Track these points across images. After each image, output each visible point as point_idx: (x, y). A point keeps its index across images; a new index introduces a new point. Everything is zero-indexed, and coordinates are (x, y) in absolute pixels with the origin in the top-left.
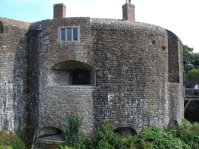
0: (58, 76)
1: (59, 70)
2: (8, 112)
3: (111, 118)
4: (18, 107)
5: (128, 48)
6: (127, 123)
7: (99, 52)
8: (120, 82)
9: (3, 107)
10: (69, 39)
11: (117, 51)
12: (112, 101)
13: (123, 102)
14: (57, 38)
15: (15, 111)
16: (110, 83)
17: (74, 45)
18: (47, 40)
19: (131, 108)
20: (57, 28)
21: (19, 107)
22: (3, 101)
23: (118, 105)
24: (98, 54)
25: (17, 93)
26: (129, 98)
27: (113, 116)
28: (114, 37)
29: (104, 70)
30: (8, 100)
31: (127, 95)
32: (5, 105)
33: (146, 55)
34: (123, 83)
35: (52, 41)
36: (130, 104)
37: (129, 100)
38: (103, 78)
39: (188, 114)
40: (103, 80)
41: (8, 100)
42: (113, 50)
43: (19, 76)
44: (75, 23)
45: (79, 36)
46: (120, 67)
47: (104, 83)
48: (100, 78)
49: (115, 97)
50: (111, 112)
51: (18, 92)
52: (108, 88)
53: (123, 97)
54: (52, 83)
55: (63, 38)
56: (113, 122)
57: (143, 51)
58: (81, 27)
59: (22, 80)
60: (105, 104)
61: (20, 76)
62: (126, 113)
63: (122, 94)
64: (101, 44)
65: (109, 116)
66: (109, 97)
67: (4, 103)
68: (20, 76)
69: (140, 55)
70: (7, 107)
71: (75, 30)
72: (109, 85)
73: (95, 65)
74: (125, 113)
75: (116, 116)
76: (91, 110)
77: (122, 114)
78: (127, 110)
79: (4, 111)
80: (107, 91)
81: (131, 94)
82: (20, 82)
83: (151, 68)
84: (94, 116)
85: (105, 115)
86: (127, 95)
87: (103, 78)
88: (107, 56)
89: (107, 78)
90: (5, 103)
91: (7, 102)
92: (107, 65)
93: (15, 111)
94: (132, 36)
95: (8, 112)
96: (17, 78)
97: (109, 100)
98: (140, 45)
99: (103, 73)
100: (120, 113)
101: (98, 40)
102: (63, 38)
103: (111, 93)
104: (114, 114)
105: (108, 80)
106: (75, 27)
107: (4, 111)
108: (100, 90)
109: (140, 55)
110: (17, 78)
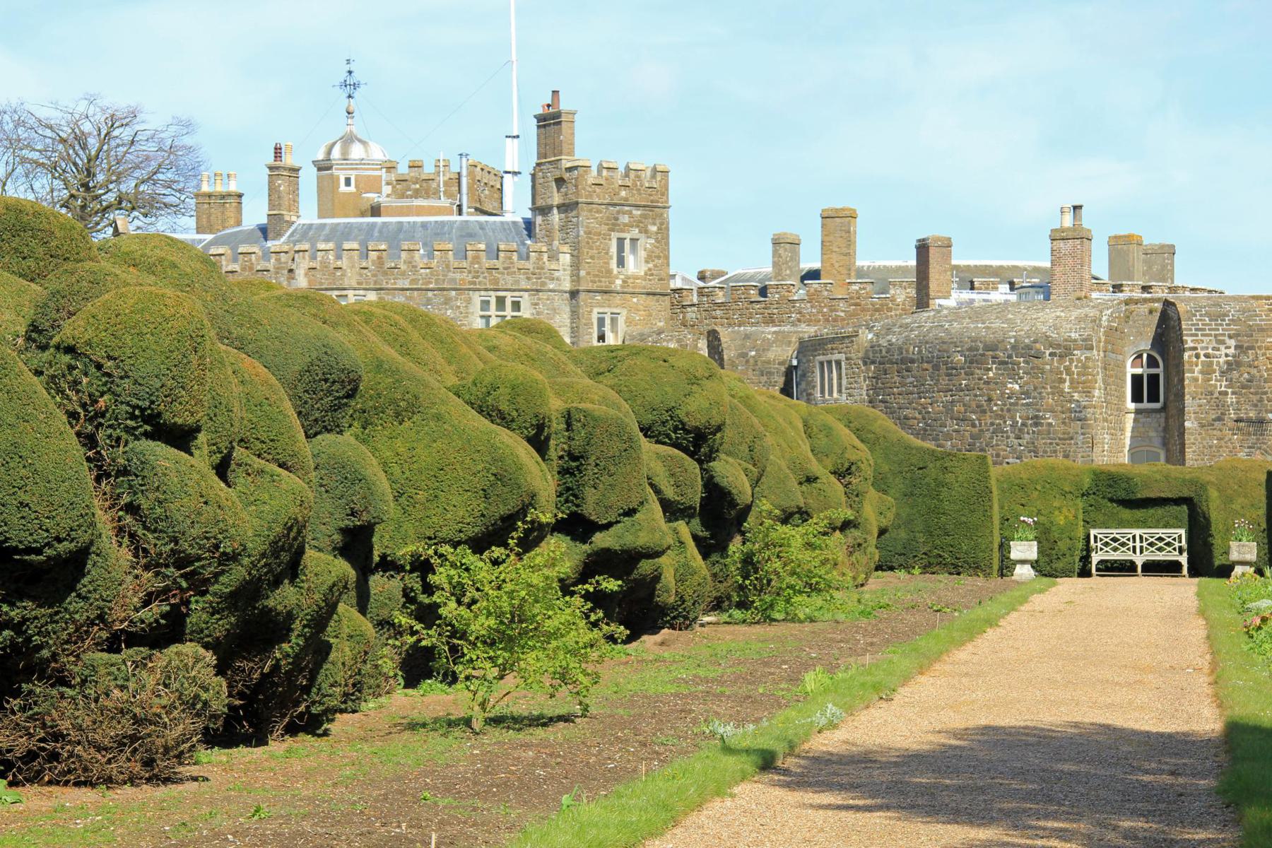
10: (831, 393)
14: (814, 387)
28: (909, 380)
33: (992, 424)
42: (906, 418)
45: (844, 382)
55: (822, 392)
57: (984, 412)
58: (847, 359)
64: (881, 401)
69: (974, 426)
71: (838, 363)
83: (1010, 460)
94: (952, 370)
98: (976, 396)
101: (874, 388)
102: (822, 392)
106: (837, 356)
109: (974, 426)
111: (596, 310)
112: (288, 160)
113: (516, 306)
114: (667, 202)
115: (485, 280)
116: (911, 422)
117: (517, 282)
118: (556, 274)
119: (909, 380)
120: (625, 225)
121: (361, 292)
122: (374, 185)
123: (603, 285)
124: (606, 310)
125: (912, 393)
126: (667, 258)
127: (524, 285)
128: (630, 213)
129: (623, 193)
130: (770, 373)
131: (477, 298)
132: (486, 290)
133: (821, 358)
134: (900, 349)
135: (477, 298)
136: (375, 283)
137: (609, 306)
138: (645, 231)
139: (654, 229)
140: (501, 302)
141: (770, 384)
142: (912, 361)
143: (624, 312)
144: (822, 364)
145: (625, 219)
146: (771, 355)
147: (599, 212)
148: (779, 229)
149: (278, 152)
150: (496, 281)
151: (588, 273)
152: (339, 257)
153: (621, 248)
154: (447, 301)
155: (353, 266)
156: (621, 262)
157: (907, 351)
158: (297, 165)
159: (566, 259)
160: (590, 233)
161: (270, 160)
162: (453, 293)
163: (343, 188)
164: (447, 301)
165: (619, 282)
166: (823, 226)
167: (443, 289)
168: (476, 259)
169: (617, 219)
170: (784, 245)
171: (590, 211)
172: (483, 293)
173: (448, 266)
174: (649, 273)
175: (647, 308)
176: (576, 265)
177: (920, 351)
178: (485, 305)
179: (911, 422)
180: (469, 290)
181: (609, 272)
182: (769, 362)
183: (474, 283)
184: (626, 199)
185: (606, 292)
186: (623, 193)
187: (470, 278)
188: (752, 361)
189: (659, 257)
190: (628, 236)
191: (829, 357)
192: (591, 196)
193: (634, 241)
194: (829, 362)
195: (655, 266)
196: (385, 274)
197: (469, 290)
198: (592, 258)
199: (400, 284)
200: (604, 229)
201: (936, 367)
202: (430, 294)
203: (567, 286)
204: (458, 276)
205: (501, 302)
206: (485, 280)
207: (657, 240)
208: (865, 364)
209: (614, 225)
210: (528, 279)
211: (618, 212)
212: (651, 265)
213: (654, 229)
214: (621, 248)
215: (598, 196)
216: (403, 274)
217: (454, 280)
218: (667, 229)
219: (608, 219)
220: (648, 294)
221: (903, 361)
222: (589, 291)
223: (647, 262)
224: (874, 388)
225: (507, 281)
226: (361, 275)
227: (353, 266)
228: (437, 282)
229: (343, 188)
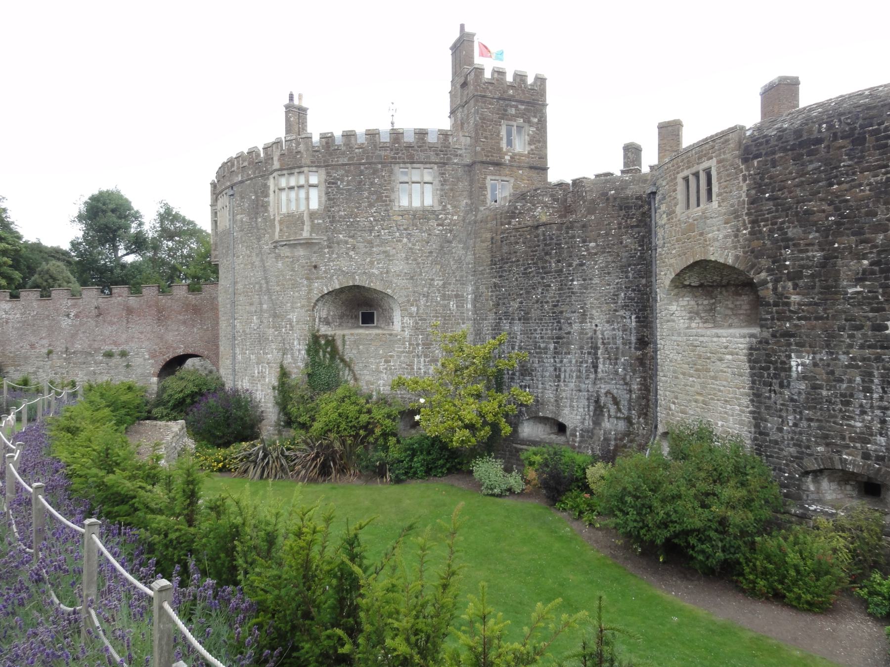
0: (706, 302)
1: (701, 286)
2: (603, 386)
3: (800, 433)
4: (624, 379)
5: (868, 192)
6: (860, 461)
7: (764, 226)
8: (834, 317)
9: (592, 376)
11: (824, 211)
12: (805, 378)
13: (844, 386)
15: (618, 386)
16: (799, 319)
17: (706, 218)
18: (664, 212)
19: (880, 408)
20: (675, 178)
21: (628, 377)
22: (593, 362)
23: (824, 393)
24: (760, 232)
25: (621, 346)
26: (871, 375)
27: (809, 426)
29: (776, 281)
30: (601, 360)
31: (864, 359)
32: (596, 372)
34: (846, 320)
35: (671, 213)
36: (875, 396)
37: (872, 382)
38: (776, 304)
39: (576, 436)
40: (777, 312)
41: (601, 360)
42: (808, 212)
43: (625, 307)
44: (705, 155)
45: (715, 189)
46: (835, 265)
47: (778, 320)
48: (768, 304)
49: (815, 365)
50: (801, 413)
51: (624, 344)
52: (793, 336)
53: (847, 367)
54: (682, 321)
56: (808, 447)
58: (719, 162)
59: (633, 317)
60: (781, 386)
61: (628, 306)
62: (859, 424)
63: (842, 357)
64: (768, 199)
65: (795, 425)
66: (793, 364)
67: (593, 367)
68: (628, 306)
70: (600, 375)
72: (796, 325)
73: (753, 266)
74: (852, 422)
75: (820, 428)
76: (745, 401)
77: (842, 425)
78: (863, 412)
79: (595, 383)
80: (789, 345)
81: (878, 359)
82: (629, 320)
84: (754, 418)
85: (783, 421)
86: (864, 359)
87: (776, 304)
88: (786, 233)
89: (788, 304)
90: (595, 367)
91: (601, 366)
92: (787, 263)
93: (618, 386)
95: (603, 386)
96: (621, 313)
97: (794, 375)
99: (775, 289)
100: (834, 423)
103: (802, 352)
104: (810, 420)
105: (791, 311)
106: (705, 165)
107: (595, 383)
108: (767, 343)
110: (621, 313)
111: (489, 178)
112: (296, 102)
114: (545, 101)
116: (814, 218)
117: (429, 157)
118: (459, 152)
119: (810, 167)
120: (513, 116)
121: (314, 169)
123: (495, 159)
124: (497, 178)
125: (817, 181)
126: (545, 142)
127: (433, 159)
128: (516, 107)
129: (511, 92)
130: (628, 208)
132: (404, 163)
133: (686, 173)
134: (798, 133)
136: (325, 162)
137: (500, 175)
138: (528, 121)
139: (536, 120)
141: (628, 217)
142: (819, 141)
143: (512, 180)
144: (686, 179)
145: (513, 111)
146: (629, 192)
147: (490, 104)
148: (628, 141)
149: (291, 97)
150: (411, 157)
151: (483, 149)
152: (298, 144)
153: (509, 134)
154: (375, 172)
155: (308, 150)
156: (510, 143)
157: (810, 131)
158: (304, 104)
160: (484, 119)
161: (287, 101)
162: (380, 166)
164: (375, 172)
165: (507, 158)
166: (659, 133)
167: (370, 163)
169: (506, 111)
170: (632, 152)
171: (484, 102)
172: (402, 165)
173: (375, 146)
174: (531, 152)
175: (529, 178)
177: (830, 127)
179: (814, 218)
180: (391, 163)
181: (500, 149)
182: (627, 198)
183: (395, 158)
184: (513, 96)
185: (497, 164)
186: (511, 92)
187: (392, 155)
188: (611, 199)
189: (539, 142)
190: (515, 124)
191: (694, 170)
192: (485, 92)
193: (519, 128)
194: (697, 175)
195: (536, 148)
196: (331, 154)
197: (391, 163)
198: (486, 138)
199: (341, 161)
200: (496, 117)
201: (859, 141)
202: (362, 167)
203: (468, 160)
204: (383, 153)
207: (537, 129)
208: (745, 160)
209: (504, 116)
210: (437, 155)
211: (507, 106)
212: (533, 147)
213: (536, 120)
214: (509, 134)
215: (491, 92)
216: (343, 153)
217: (380, 156)
218: (545, 121)
219: (499, 109)
220: (531, 168)
221: (801, 145)
222: (483, 163)
223: (530, 144)
224: (758, 186)
226: (314, 156)
227: (308, 150)
228: (367, 158)
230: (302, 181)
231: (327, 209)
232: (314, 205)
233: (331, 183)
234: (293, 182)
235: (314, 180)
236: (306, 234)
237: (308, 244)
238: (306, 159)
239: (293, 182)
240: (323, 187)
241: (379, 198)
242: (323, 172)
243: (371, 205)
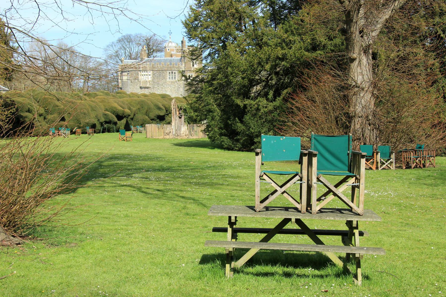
113: (175, 73)
115: (169, 69)
122: (173, 50)
131: (168, 72)
135: (168, 72)
140: (172, 72)
156: (193, 66)
159: (184, 65)
163: (168, 51)
164: (163, 72)
168: (168, 65)
176: (185, 66)
178: (170, 73)
181: (191, 67)
205: (172, 72)
206: (169, 69)
225: (173, 69)
229: (168, 51)
230: (147, 74)
231: (153, 80)
232: (150, 79)
233: (154, 74)
234: (144, 73)
235: (149, 74)
236: (148, 85)
237: (148, 88)
238: (148, 69)
239: (144, 73)
240: (151, 76)
241: (164, 78)
242: (152, 71)
243: (162, 80)
